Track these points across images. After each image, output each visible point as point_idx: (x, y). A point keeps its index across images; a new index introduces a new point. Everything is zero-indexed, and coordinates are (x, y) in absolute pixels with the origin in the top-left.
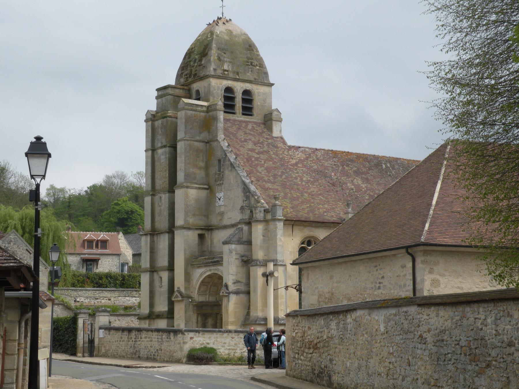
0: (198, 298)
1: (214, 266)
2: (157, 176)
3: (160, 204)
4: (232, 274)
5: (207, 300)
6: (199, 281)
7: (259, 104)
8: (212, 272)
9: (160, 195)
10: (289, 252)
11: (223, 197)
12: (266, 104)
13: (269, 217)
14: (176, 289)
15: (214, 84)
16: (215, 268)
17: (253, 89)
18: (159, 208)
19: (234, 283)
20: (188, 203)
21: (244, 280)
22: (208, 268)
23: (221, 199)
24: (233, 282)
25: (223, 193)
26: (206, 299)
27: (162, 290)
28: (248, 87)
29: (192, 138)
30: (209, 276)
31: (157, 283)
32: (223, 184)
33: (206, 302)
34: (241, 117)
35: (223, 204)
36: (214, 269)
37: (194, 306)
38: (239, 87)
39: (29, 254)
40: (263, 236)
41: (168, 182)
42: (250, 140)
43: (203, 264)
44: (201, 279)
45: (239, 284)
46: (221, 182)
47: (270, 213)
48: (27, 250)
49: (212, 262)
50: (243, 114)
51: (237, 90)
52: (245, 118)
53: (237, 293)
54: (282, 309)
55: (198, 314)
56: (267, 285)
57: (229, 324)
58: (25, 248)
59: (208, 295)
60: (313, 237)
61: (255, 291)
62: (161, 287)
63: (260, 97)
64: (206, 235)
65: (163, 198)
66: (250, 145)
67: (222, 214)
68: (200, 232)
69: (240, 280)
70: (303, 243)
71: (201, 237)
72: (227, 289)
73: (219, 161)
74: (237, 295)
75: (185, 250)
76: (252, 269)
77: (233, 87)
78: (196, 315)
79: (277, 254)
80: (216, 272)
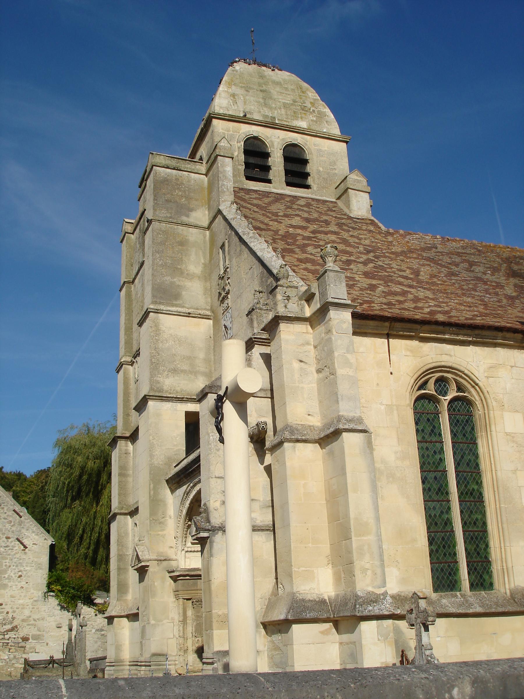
7: (321, 169)
10: (383, 407)
12: (336, 172)
15: (221, 131)
17: (306, 144)
20: (160, 345)
28: (294, 139)
29: (171, 217)
34: (282, 189)
39: (18, 517)
42: (297, 215)
48: (14, 511)
50: (288, 184)
51: (272, 142)
52: (291, 191)
54: (367, 566)
56: (222, 440)
57: (215, 625)
58: (12, 507)
60: (450, 369)
63: (322, 158)
66: (297, 221)
77: (262, 137)
79: (337, 402)
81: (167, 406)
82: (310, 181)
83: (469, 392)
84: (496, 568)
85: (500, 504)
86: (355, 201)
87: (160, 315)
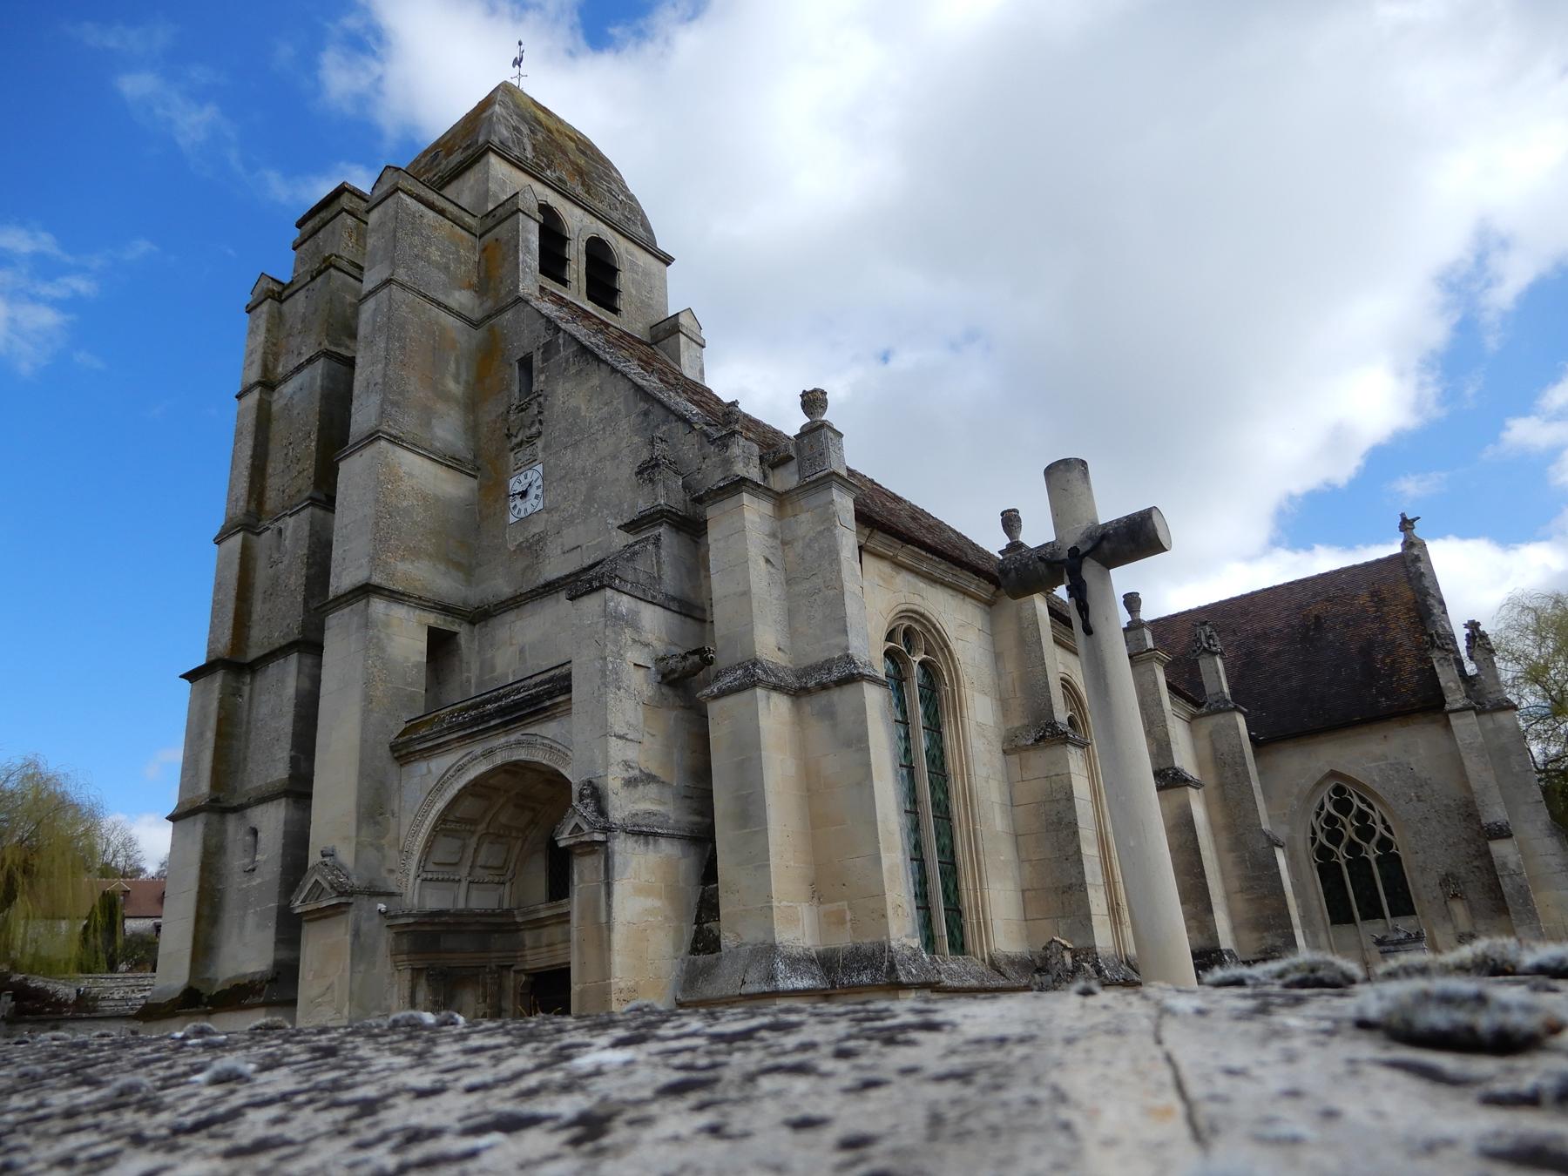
0: (418, 896)
1: (507, 733)
2: (275, 465)
3: (276, 556)
4: (621, 737)
5: (461, 905)
6: (427, 813)
8: (499, 759)
9: (279, 524)
11: (540, 482)
13: (786, 479)
14: (314, 858)
16: (513, 737)
18: (271, 571)
19: (630, 783)
21: (676, 778)
22: (478, 749)
23: (533, 492)
24: (626, 775)
25: (539, 468)
26: (455, 899)
27: (257, 881)
30: (476, 788)
31: (236, 861)
32: (540, 433)
33: (458, 914)
35: (540, 506)
36: (508, 746)
37: (400, 932)
38: (578, 224)
40: (767, 561)
41: (312, 470)
43: (450, 730)
44: (440, 805)
45: (652, 790)
46: (534, 430)
47: (793, 466)
49: (501, 712)
52: (596, 310)
53: (643, 833)
55: (416, 973)
59: (464, 884)
61: (751, 813)
62: (254, 870)
64: (463, 640)
65: (288, 533)
67: (533, 548)
68: (433, 619)
69: (653, 768)
70: (890, 636)
71: (440, 645)
72: (602, 812)
73: (526, 364)
74: (647, 843)
75: (368, 683)
76: (722, 716)
78: (407, 975)
80: (521, 755)
81: (399, 612)
82: (621, 303)
83: (936, 656)
84: (970, 920)
85: (974, 825)
86: (686, 354)
87: (400, 451)
